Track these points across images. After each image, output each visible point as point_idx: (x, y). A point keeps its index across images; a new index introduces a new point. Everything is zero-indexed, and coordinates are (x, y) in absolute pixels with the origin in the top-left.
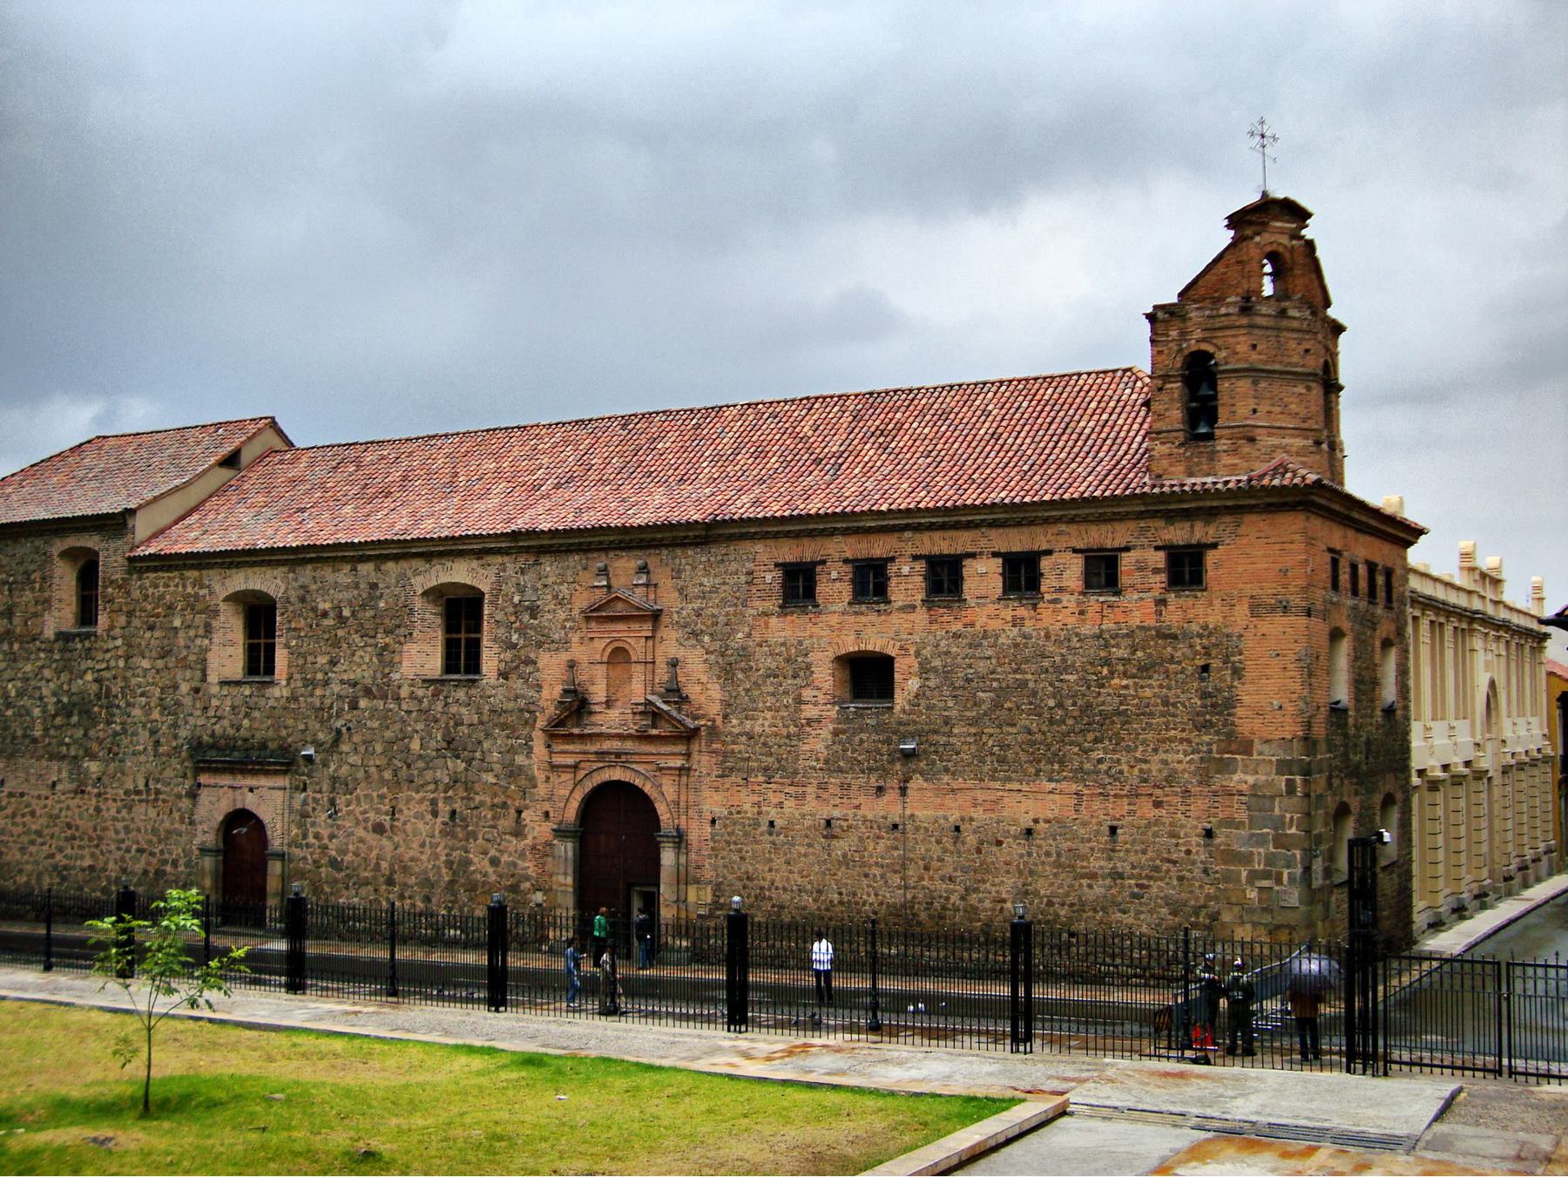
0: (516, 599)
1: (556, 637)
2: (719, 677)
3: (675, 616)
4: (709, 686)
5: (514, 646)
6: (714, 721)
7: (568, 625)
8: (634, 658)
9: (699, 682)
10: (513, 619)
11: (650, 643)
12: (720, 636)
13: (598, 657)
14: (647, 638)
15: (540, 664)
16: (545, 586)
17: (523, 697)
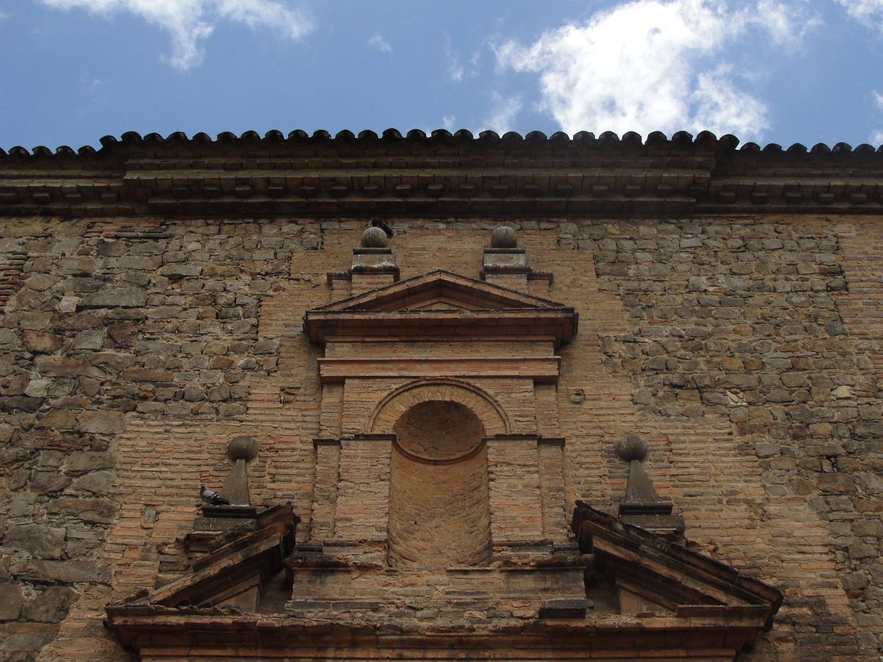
0: (69, 303)
1: (196, 385)
2: (802, 488)
3: (619, 348)
4: (772, 508)
5: (32, 405)
6: (818, 603)
7: (240, 361)
8: (493, 427)
9: (732, 497)
10: (46, 343)
11: (548, 396)
12: (775, 394)
13: (362, 425)
14: (540, 382)
15: (118, 450)
16: (176, 278)
17: (30, 540)
